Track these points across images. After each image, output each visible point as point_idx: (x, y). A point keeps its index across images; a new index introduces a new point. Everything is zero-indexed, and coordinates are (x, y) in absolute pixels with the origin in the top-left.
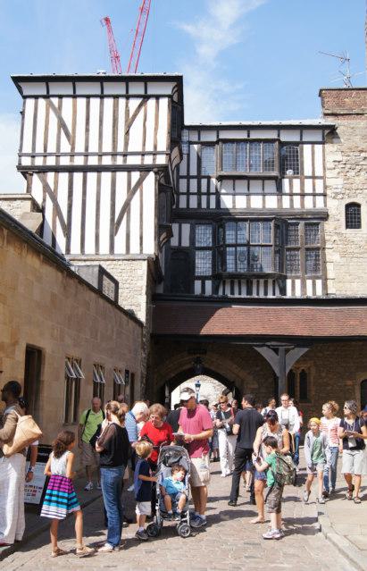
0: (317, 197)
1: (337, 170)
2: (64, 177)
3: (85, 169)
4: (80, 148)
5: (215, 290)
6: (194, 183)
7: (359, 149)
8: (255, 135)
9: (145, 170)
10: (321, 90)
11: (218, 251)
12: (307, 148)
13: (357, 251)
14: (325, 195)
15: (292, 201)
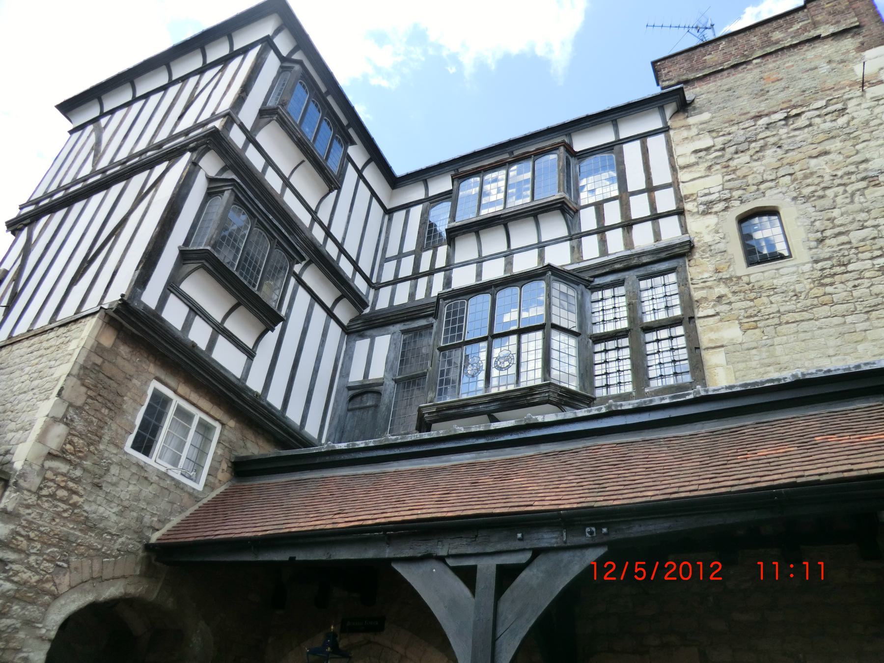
0: (662, 221)
1: (703, 166)
7: (752, 114)
10: (654, 63)
13: (790, 306)
14: (680, 212)
15: (603, 243)
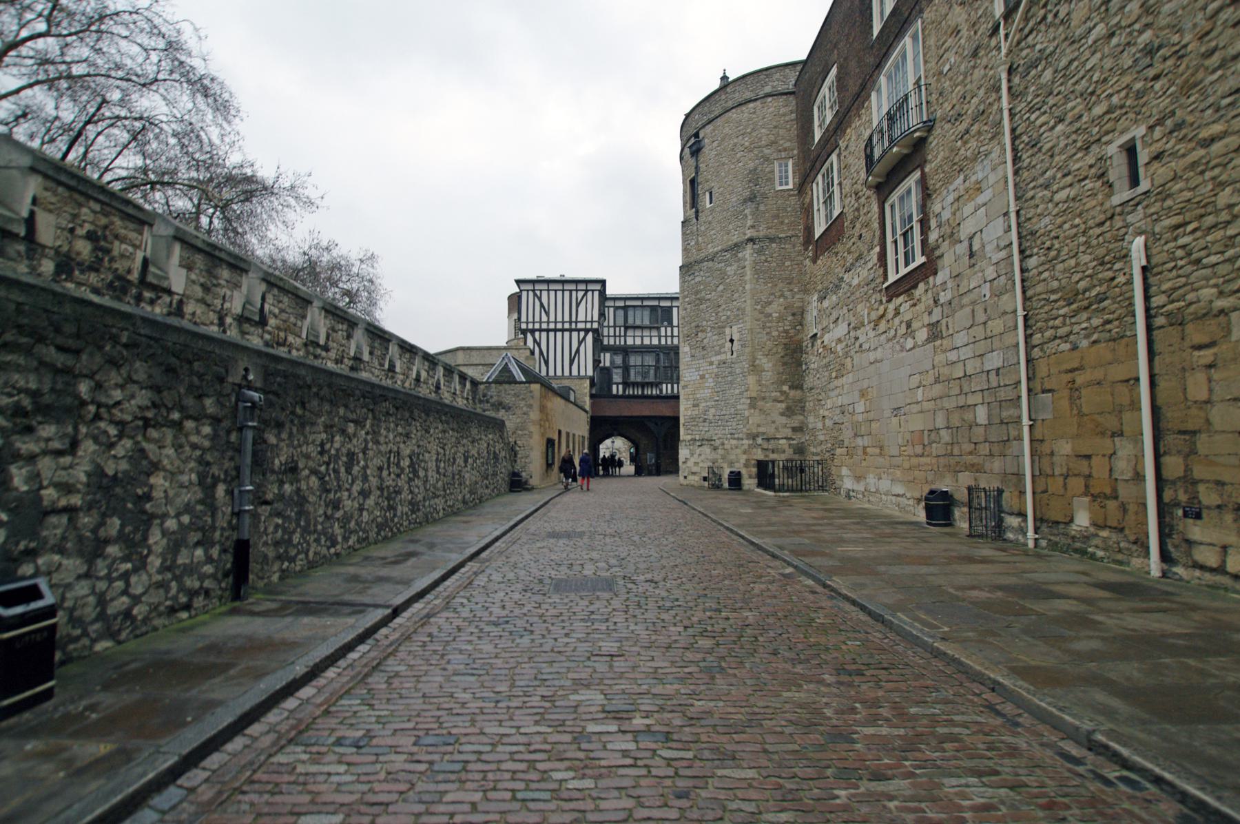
2: (544, 334)
3: (555, 330)
4: (552, 319)
5: (624, 390)
6: (612, 330)
8: (645, 303)
9: (587, 331)
11: (626, 369)
12: (675, 310)
